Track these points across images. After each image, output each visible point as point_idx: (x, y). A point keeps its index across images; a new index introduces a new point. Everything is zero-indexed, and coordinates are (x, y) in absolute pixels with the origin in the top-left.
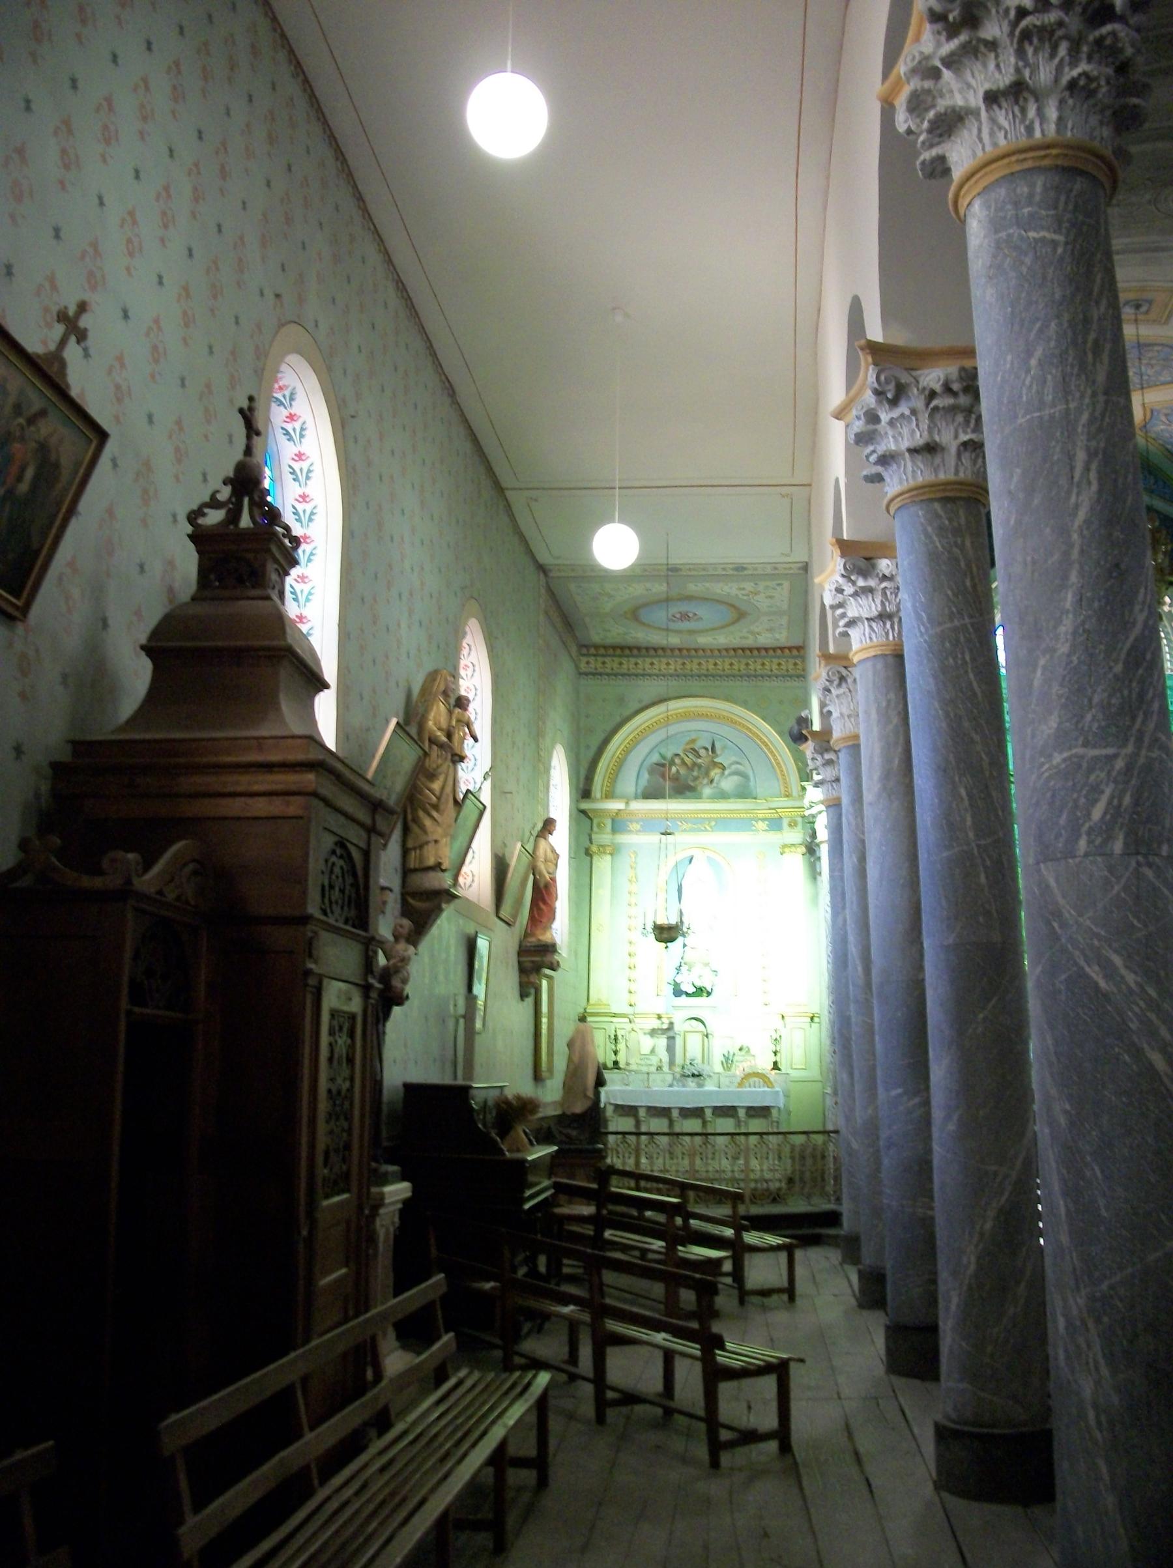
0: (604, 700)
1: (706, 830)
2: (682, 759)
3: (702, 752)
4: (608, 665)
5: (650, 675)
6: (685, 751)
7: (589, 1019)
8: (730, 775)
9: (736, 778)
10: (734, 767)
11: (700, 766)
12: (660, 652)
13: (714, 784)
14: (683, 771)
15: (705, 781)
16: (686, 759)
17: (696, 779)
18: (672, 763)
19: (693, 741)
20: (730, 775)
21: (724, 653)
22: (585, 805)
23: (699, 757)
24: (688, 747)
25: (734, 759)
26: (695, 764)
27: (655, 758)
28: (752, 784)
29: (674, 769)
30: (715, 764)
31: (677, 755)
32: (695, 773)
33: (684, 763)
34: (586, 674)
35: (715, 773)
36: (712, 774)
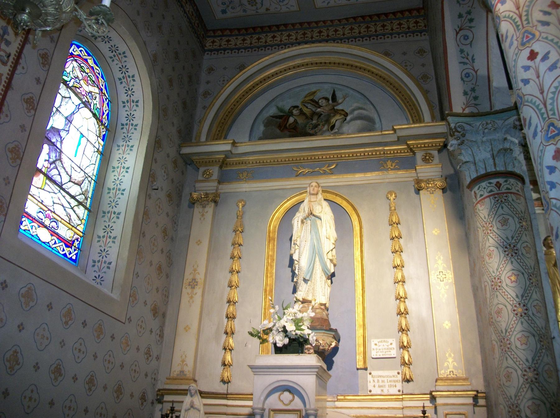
0: (225, 68)
1: (325, 173)
3: (323, 102)
4: (233, 43)
5: (272, 46)
6: (304, 103)
7: (167, 398)
8: (352, 120)
9: (359, 122)
10: (356, 112)
11: (320, 115)
12: (282, 28)
13: (335, 130)
14: (301, 121)
16: (305, 110)
17: (316, 126)
18: (290, 114)
19: (314, 93)
20: (352, 120)
21: (344, 22)
22: (186, 150)
23: (320, 107)
24: (307, 99)
25: (355, 105)
26: (314, 113)
27: (273, 111)
28: (378, 125)
29: (291, 120)
30: (336, 112)
32: (314, 122)
33: (302, 113)
34: (211, 51)
35: (336, 119)
36: (333, 120)
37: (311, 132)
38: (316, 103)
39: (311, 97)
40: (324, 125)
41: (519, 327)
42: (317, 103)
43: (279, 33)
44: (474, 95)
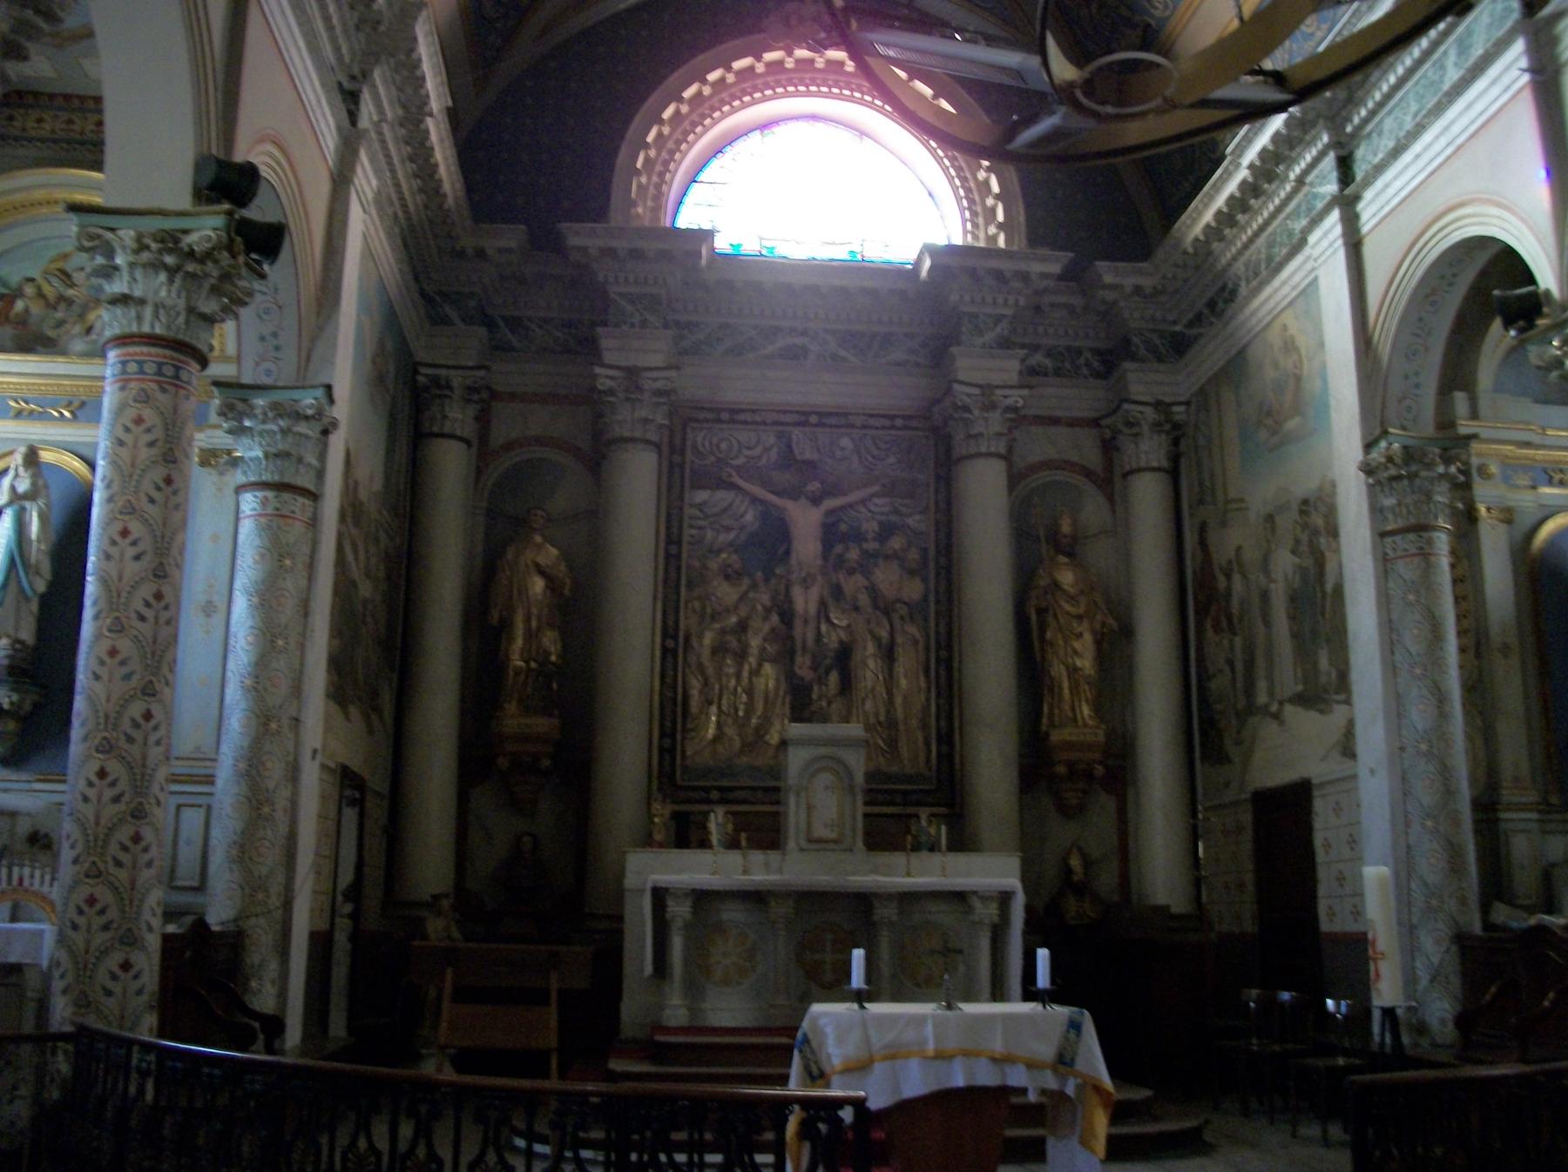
2: (39, 288)
6: (46, 272)
11: (69, 302)
15: (77, 329)
16: (47, 289)
17: (60, 324)
18: (18, 293)
23: (73, 285)
24: (53, 266)
26: (61, 298)
29: (19, 305)
31: (32, 280)
32: (59, 315)
33: (40, 295)
36: (92, 316)
37: (51, 333)
38: (65, 276)
39: (60, 265)
40: (74, 323)
41: (243, 705)
42: (68, 276)
43: (22, 111)
44: (275, 342)
